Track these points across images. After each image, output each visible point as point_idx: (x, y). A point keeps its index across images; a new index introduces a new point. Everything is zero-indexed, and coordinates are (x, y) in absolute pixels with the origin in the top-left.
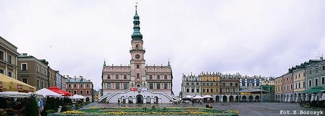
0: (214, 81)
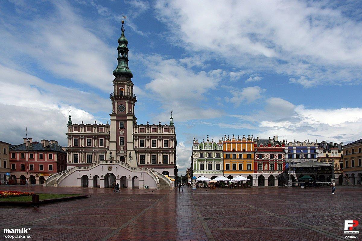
0: (244, 151)
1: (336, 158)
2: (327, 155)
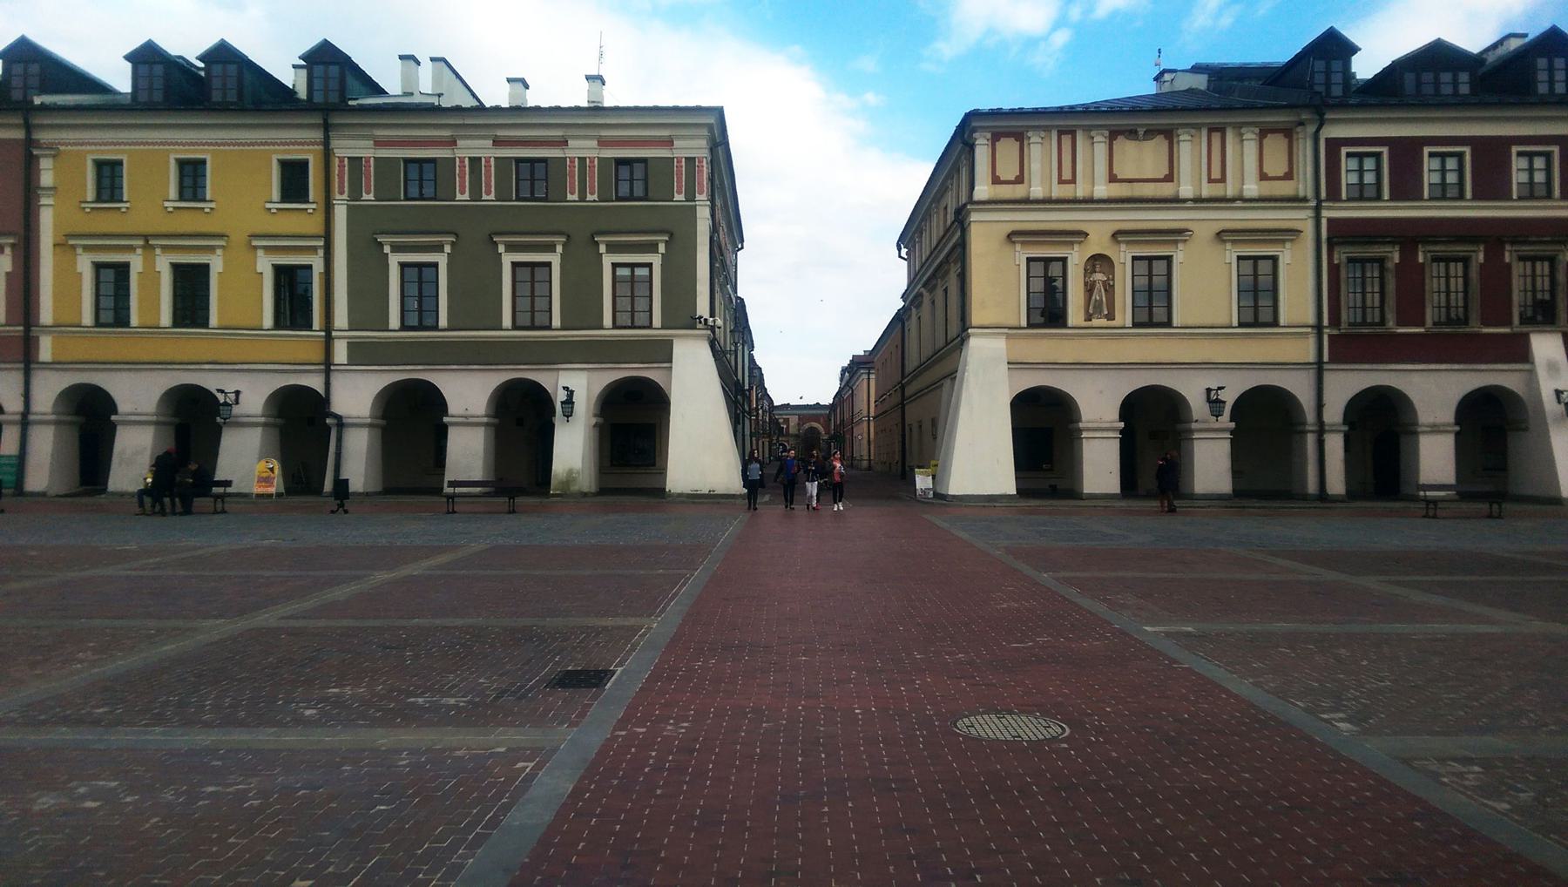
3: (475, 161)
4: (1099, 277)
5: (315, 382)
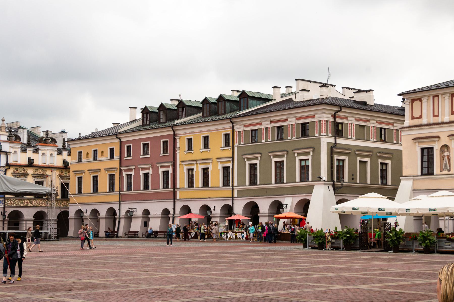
1: (52, 168)
2: (29, 159)
3: (266, 128)
4: (446, 154)
5: (230, 203)
